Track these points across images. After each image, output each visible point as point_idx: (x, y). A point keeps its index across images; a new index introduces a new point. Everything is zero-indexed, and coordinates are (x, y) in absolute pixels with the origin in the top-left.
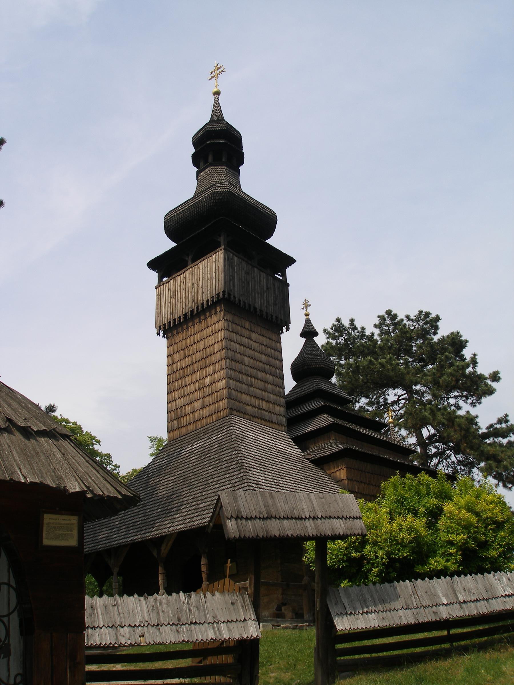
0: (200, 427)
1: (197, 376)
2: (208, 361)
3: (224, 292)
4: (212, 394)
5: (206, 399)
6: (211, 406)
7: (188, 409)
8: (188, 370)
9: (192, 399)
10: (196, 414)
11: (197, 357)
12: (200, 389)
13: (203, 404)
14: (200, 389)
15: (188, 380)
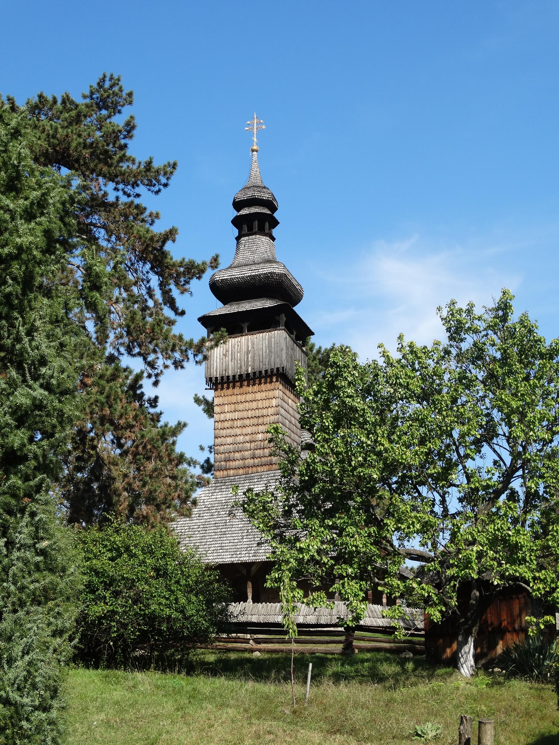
0: (250, 472)
1: (249, 430)
2: (260, 420)
3: (283, 368)
4: (263, 449)
5: (258, 452)
6: (263, 459)
7: (237, 455)
8: (239, 423)
9: (242, 447)
10: (247, 461)
11: (250, 414)
12: (251, 442)
13: (254, 454)
14: (251, 442)
15: (238, 431)
